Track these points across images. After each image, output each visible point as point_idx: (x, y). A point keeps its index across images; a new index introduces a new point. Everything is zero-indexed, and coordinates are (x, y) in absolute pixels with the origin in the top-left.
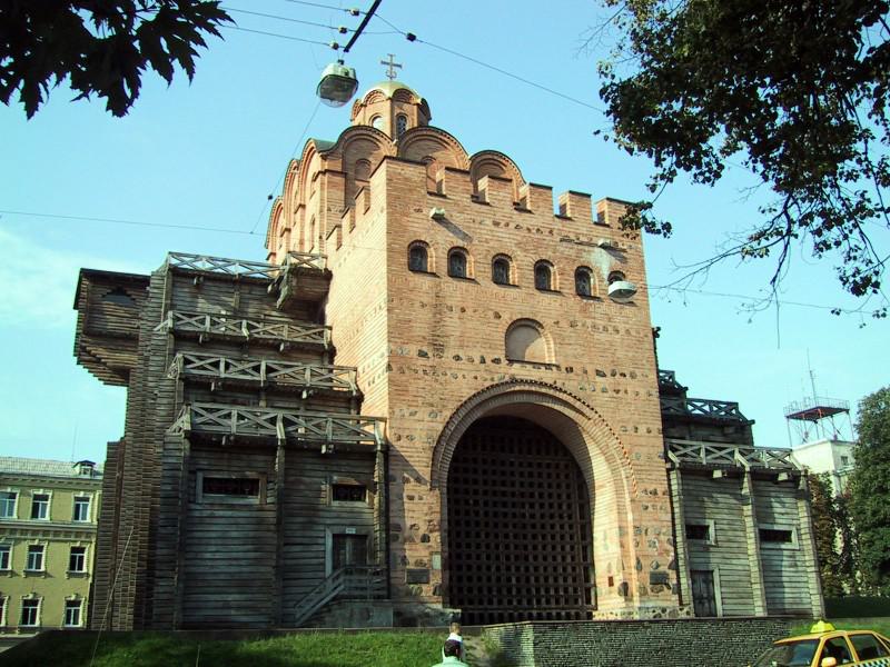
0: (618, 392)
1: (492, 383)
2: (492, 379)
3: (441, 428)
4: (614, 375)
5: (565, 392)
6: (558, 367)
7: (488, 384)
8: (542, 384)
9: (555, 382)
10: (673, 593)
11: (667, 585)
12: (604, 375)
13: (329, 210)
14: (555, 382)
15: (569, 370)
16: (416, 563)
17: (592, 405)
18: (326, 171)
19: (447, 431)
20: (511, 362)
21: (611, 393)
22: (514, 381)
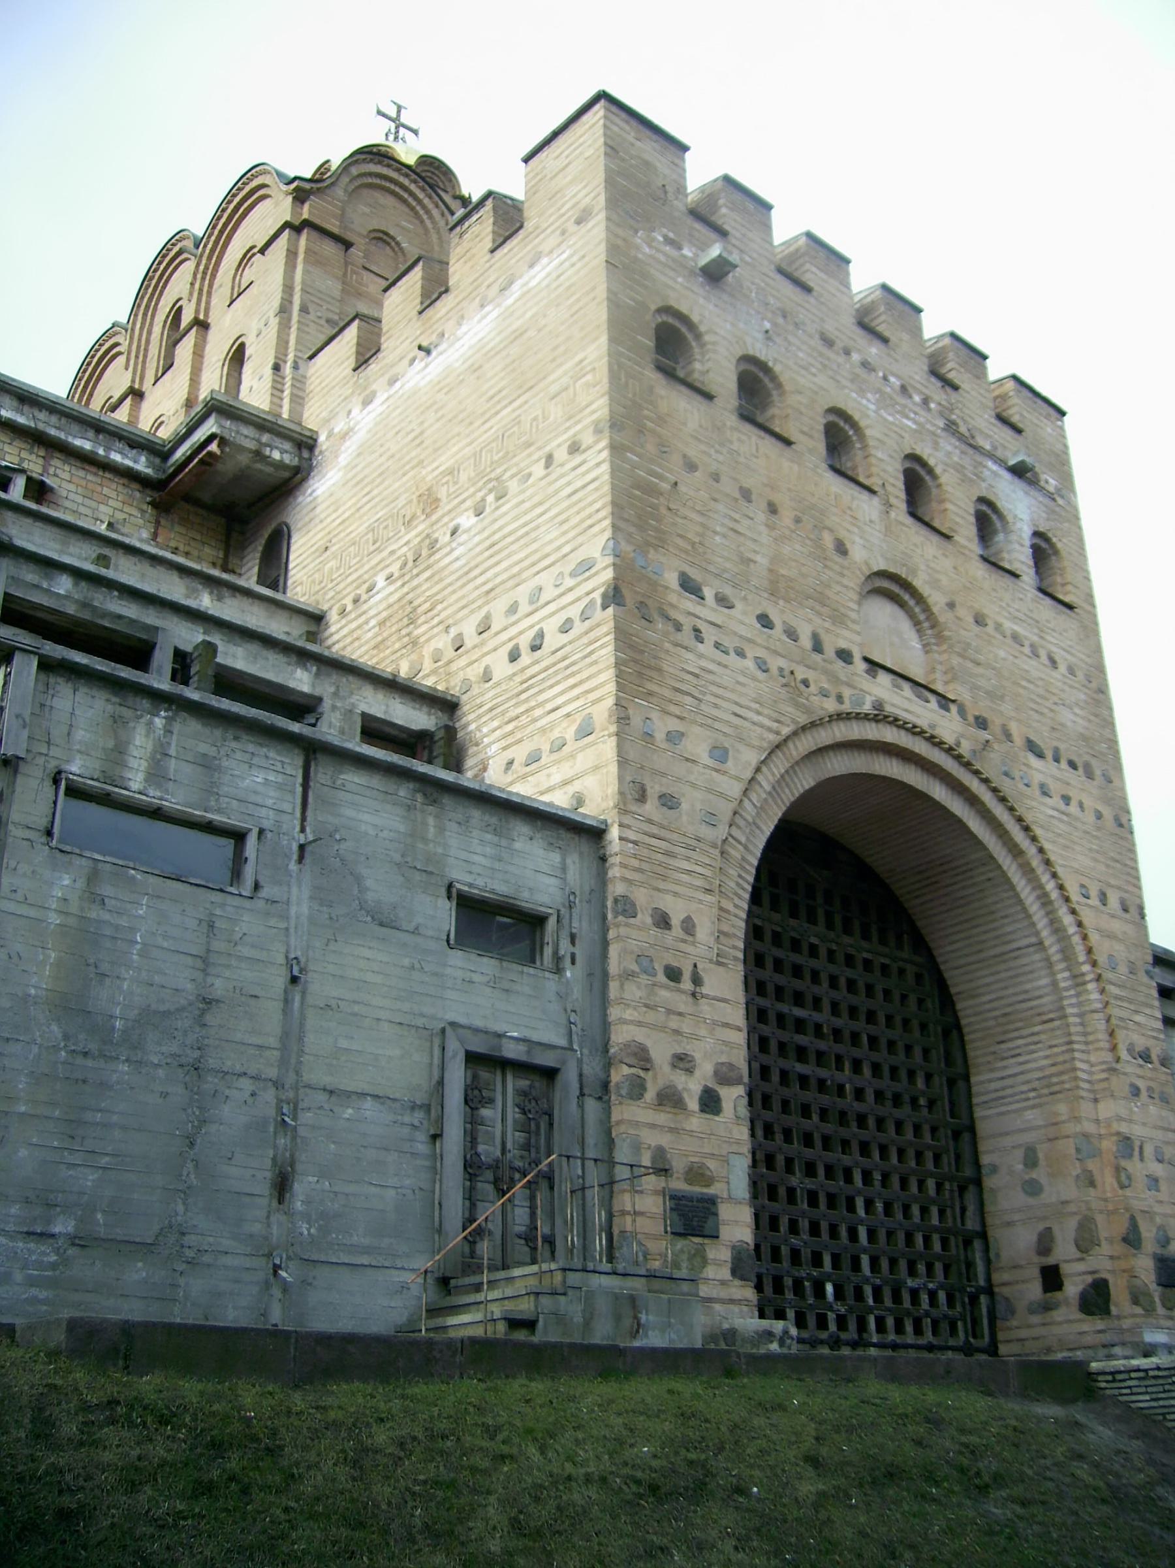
2: (840, 699)
3: (736, 790)
5: (977, 773)
6: (962, 712)
7: (831, 706)
9: (958, 744)
12: (1040, 755)
13: (304, 309)
17: (1029, 818)
18: (306, 224)
19: (746, 803)
21: (1056, 801)
22: (880, 716)
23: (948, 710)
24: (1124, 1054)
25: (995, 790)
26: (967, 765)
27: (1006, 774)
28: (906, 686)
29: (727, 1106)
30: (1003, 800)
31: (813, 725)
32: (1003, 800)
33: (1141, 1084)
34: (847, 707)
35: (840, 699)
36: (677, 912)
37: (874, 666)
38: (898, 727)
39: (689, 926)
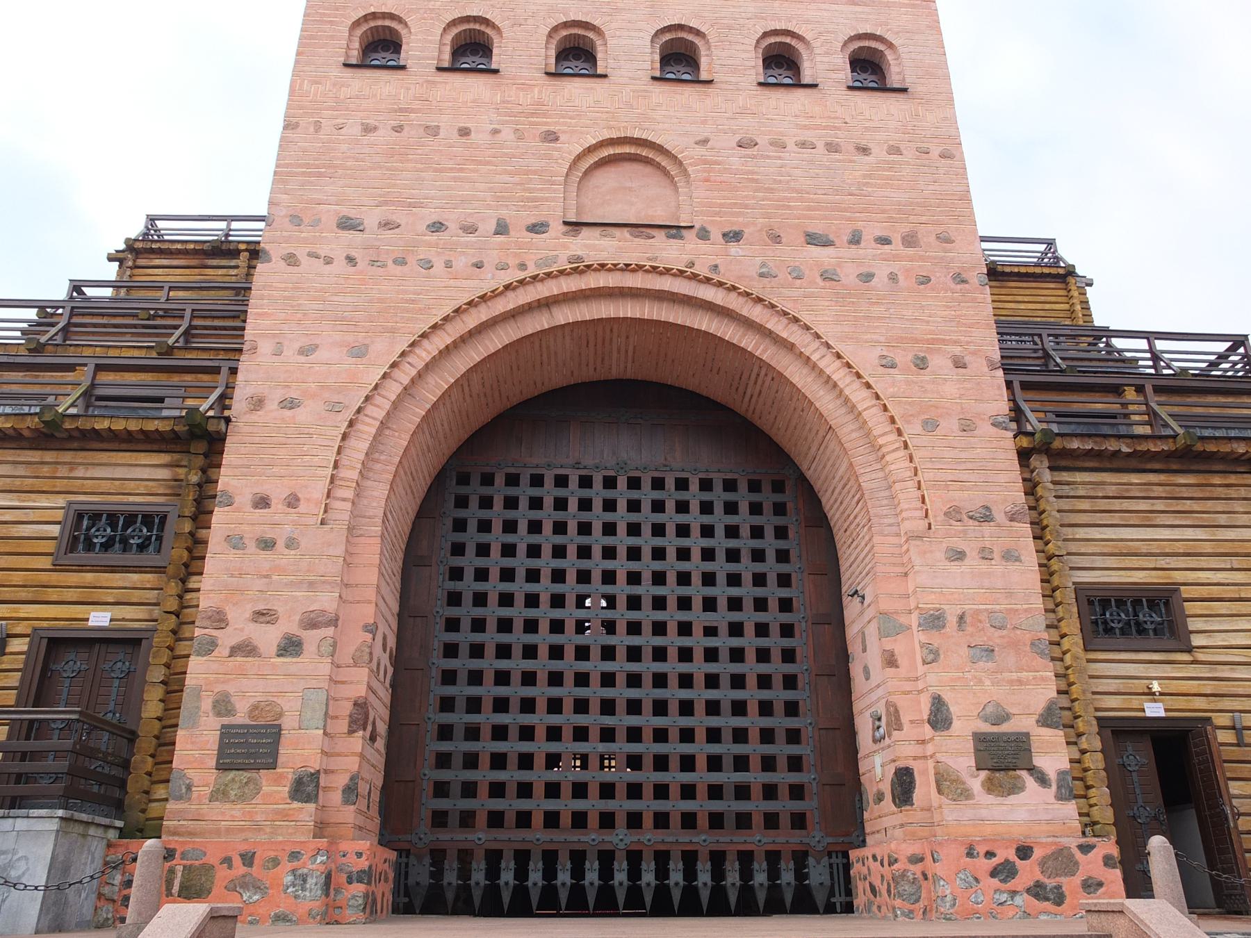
0: (868, 277)
1: (521, 275)
2: (523, 266)
4: (855, 240)
9: (692, 265)
10: (1059, 797)
11: (1031, 769)
12: (827, 243)
14: (692, 265)
16: (255, 707)
20: (575, 226)
22: (581, 268)
23: (681, 238)
24: (937, 518)
27: (762, 275)
28: (625, 233)
29: (310, 647)
31: (483, 298)
33: (961, 545)
34: (532, 270)
35: (523, 266)
36: (277, 493)
38: (610, 270)
39: (293, 501)
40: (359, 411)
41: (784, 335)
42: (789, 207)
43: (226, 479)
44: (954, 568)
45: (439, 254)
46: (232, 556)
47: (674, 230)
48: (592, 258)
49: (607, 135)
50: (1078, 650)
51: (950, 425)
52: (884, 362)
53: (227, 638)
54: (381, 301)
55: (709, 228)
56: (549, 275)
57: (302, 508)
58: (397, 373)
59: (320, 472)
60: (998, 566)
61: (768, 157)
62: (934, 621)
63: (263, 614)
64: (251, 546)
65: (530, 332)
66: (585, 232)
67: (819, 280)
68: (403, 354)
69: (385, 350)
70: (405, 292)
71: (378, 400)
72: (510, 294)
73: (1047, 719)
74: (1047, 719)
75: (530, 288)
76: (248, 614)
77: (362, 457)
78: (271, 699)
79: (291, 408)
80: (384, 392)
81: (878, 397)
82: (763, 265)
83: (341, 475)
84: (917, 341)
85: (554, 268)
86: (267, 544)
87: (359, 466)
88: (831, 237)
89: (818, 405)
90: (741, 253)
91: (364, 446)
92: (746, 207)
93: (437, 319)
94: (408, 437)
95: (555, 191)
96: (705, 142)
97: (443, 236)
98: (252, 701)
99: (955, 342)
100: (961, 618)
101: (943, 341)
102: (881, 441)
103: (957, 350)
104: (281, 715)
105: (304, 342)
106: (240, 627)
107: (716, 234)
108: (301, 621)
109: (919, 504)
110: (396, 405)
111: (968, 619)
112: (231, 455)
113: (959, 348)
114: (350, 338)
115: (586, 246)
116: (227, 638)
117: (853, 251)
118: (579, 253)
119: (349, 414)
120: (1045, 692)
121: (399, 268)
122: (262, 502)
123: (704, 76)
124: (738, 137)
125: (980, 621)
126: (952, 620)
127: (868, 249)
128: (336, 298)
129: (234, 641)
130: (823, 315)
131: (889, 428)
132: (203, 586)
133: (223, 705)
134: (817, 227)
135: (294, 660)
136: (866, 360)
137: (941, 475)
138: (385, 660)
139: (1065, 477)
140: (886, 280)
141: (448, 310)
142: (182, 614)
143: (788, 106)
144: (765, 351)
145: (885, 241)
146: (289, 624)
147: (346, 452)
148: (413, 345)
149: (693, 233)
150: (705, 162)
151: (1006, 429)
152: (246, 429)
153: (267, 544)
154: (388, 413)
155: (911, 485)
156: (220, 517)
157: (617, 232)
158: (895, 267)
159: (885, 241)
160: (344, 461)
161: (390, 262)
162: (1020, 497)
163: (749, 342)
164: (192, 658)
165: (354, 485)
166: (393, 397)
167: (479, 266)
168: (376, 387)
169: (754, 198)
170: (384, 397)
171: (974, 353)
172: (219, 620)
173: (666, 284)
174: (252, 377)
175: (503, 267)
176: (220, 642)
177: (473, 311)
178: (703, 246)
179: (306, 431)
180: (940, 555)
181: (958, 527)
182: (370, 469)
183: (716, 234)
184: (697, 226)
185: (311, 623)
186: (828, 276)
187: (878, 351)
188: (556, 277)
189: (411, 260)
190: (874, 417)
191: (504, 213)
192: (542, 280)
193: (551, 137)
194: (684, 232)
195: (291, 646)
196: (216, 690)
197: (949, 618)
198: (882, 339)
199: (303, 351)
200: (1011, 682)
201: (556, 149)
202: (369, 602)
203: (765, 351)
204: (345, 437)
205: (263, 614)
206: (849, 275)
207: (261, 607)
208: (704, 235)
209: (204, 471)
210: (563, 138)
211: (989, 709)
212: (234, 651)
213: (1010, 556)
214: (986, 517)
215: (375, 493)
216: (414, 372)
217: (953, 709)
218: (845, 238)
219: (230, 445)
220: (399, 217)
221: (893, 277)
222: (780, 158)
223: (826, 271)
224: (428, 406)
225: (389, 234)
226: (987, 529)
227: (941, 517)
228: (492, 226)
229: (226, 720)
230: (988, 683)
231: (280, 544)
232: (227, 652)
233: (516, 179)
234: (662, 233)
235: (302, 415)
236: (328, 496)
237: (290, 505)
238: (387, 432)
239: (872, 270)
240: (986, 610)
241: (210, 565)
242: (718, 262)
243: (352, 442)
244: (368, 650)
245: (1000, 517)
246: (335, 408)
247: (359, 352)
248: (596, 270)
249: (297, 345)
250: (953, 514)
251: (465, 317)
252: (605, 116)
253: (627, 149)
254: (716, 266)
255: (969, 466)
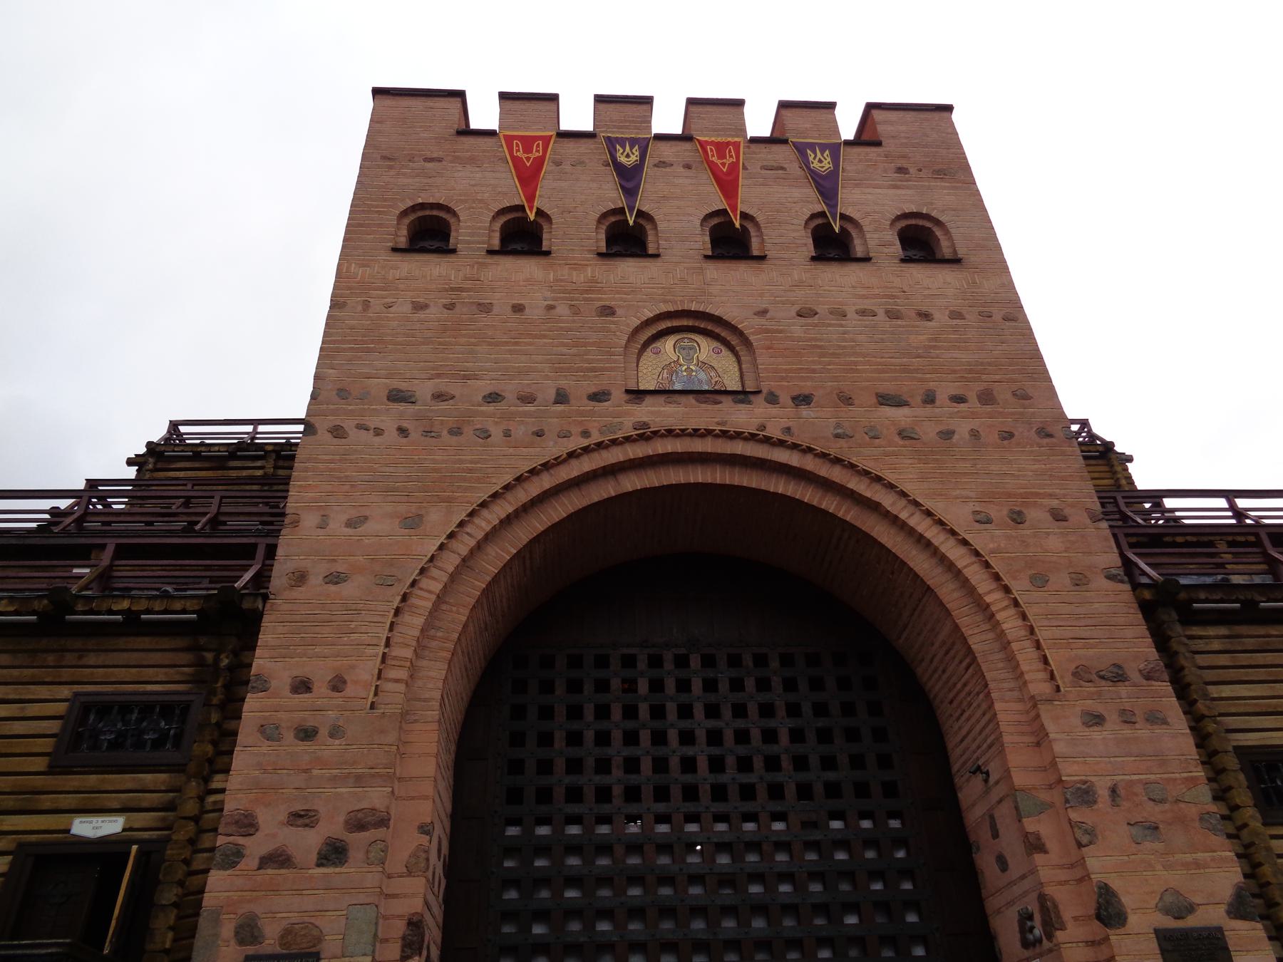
1: (585, 442)
2: (586, 434)
4: (930, 399)
7: (577, 442)
8: (724, 434)
9: (763, 427)
14: (763, 427)
15: (803, 400)
16: (287, 932)
22: (646, 435)
23: (749, 403)
24: (1064, 681)
25: (824, 456)
26: (781, 443)
27: (837, 436)
28: (691, 399)
29: (356, 855)
30: (837, 461)
31: (546, 466)
32: (837, 461)
33: (1099, 708)
34: (596, 437)
35: (586, 434)
36: (320, 673)
37: (637, 395)
38: (677, 436)
39: (338, 684)
40: (414, 584)
41: (868, 494)
42: (857, 371)
43: (261, 662)
44: (1096, 734)
45: (496, 423)
46: (265, 747)
47: (742, 396)
48: (658, 423)
49: (664, 308)
50: (1256, 824)
51: (1060, 580)
52: (978, 517)
53: (256, 847)
54: (435, 470)
55: (778, 392)
56: (614, 442)
57: (350, 690)
58: (454, 544)
59: (370, 651)
60: (1143, 732)
61: (830, 325)
62: (1085, 795)
63: (301, 816)
64: (289, 736)
65: (596, 500)
66: (649, 400)
67: (897, 439)
68: (461, 524)
69: (439, 520)
70: (461, 462)
71: (434, 572)
72: (574, 462)
73: (1238, 909)
74: (1238, 909)
75: (595, 455)
76: (283, 817)
77: (417, 633)
78: (306, 919)
79: (337, 583)
80: (440, 564)
81: (977, 554)
82: (838, 425)
83: (394, 654)
84: (1009, 495)
85: (619, 435)
86: (306, 734)
87: (414, 643)
88: (905, 397)
89: (911, 564)
90: (813, 415)
91: (419, 621)
92: (814, 371)
93: (497, 488)
94: (467, 612)
95: (615, 361)
96: (763, 313)
97: (501, 406)
98: (284, 924)
99: (1051, 496)
100: (1113, 791)
101: (1037, 495)
102: (988, 599)
103: (1055, 503)
104: (319, 940)
105: (353, 513)
106: (272, 831)
107: (785, 398)
108: (346, 822)
109: (1041, 666)
110: (454, 577)
111: (1122, 792)
112: (269, 634)
113: (1056, 502)
114: (402, 508)
115: (652, 413)
116: (256, 847)
117: (928, 410)
118: (645, 419)
119: (403, 588)
120: (1226, 877)
121: (455, 438)
122: (302, 686)
123: (755, 253)
124: (797, 307)
125: (1136, 795)
126: (1103, 793)
127: (944, 408)
128: (387, 469)
129: (264, 850)
130: (907, 474)
131: (994, 585)
132: (229, 786)
133: (248, 932)
134: (888, 387)
135: (337, 870)
136: (958, 516)
137: (1058, 633)
138: (439, 871)
139: (1196, 631)
140: (967, 436)
141: (508, 478)
142: (204, 821)
143: (839, 281)
144: (847, 511)
145: (959, 399)
146: (331, 826)
147: (397, 629)
148: (472, 514)
149: (759, 400)
150: (767, 331)
151: (1122, 582)
152: (286, 607)
153: (306, 734)
154: (445, 587)
155: (1027, 643)
156: (252, 704)
157: (683, 399)
158: (975, 424)
159: (959, 399)
160: (396, 638)
161: (445, 433)
162: (1152, 653)
163: (830, 504)
164: (212, 872)
165: (408, 664)
166: (451, 569)
167: (539, 434)
168: (432, 559)
169: (820, 363)
170: (441, 569)
171: (1072, 506)
172: (248, 825)
173: (739, 448)
174: (292, 550)
175: (566, 435)
176: (247, 852)
177: (535, 479)
178: (774, 410)
179: (354, 607)
180: (1077, 721)
181: (1091, 689)
182: (425, 647)
183: (785, 398)
184: (765, 391)
185: (358, 824)
186: (904, 434)
187: (971, 507)
188: (621, 443)
189: (468, 431)
190: (975, 575)
191: (563, 383)
192: (607, 447)
193: (608, 311)
194: (752, 397)
195: (334, 853)
196: (240, 911)
197: (1100, 792)
198: (972, 494)
199: (350, 524)
200: (1186, 865)
201: (614, 323)
202: (426, 798)
203: (847, 511)
204: (397, 612)
205: (301, 816)
206: (929, 432)
207: (298, 807)
208: (772, 399)
209: (236, 653)
210: (619, 311)
211: (1169, 899)
212: (265, 861)
213: (1155, 718)
214: (1117, 676)
215: (433, 674)
216: (472, 543)
217: (1125, 900)
218: (919, 399)
219: (267, 622)
220: (453, 388)
221: (975, 434)
222: (842, 326)
223: (903, 430)
224: (489, 579)
225: (443, 406)
226: (1123, 690)
227: (1069, 678)
228: (552, 394)
229: (251, 950)
230: (1159, 867)
231: (323, 732)
232: (256, 863)
233: (574, 350)
234: (730, 398)
235: (348, 590)
236: (379, 678)
237: (335, 688)
238: (444, 607)
239: (951, 427)
240: (1140, 781)
241: (240, 760)
242: (790, 424)
243: (406, 618)
244: (424, 855)
245: (1135, 677)
246: (385, 582)
247: (413, 522)
248: (663, 436)
249: (344, 517)
250: (1080, 674)
251: (526, 485)
252: (660, 292)
253: (685, 322)
254: (789, 429)
255: (1089, 622)
